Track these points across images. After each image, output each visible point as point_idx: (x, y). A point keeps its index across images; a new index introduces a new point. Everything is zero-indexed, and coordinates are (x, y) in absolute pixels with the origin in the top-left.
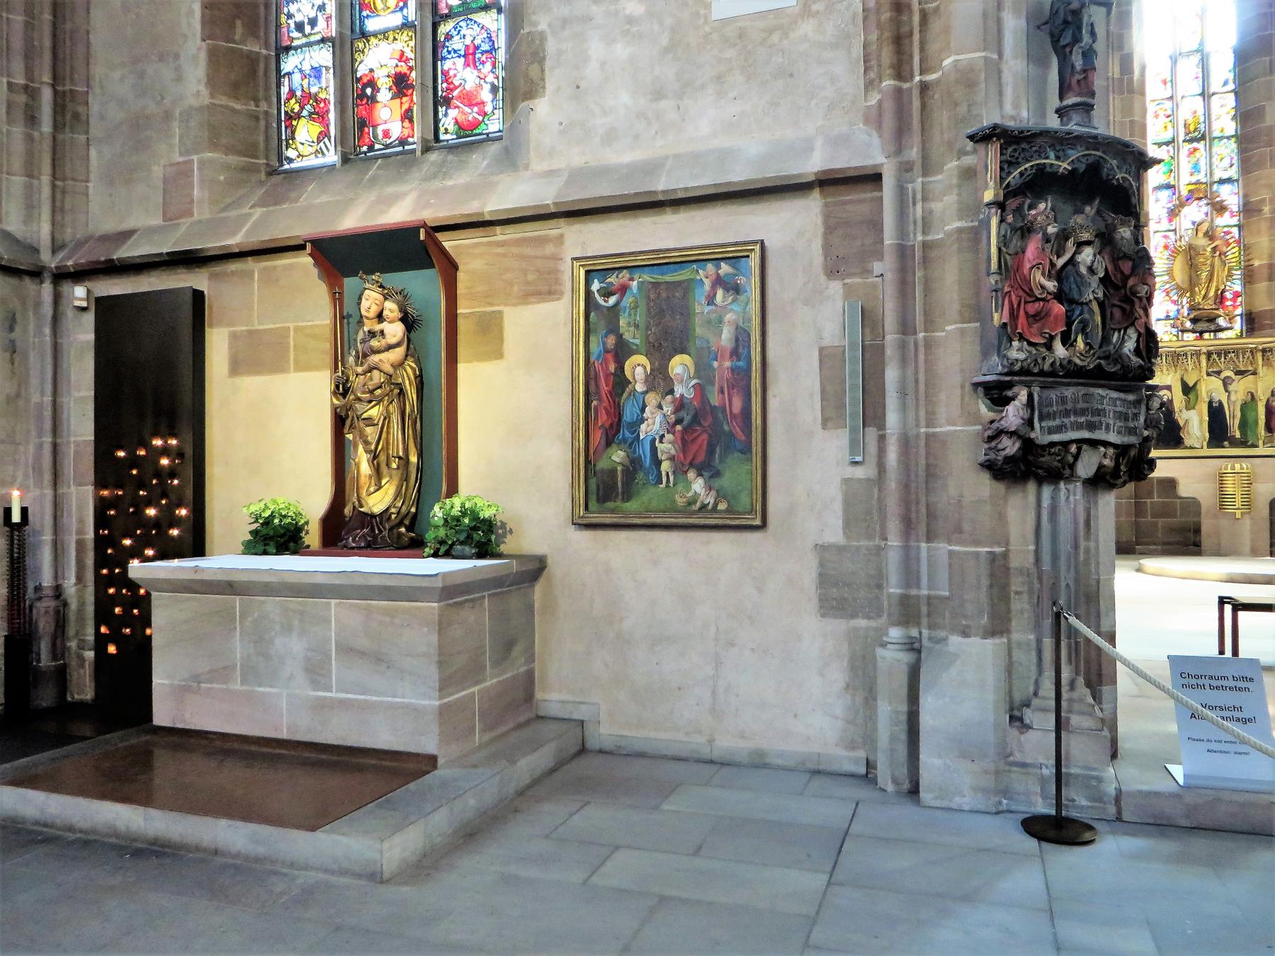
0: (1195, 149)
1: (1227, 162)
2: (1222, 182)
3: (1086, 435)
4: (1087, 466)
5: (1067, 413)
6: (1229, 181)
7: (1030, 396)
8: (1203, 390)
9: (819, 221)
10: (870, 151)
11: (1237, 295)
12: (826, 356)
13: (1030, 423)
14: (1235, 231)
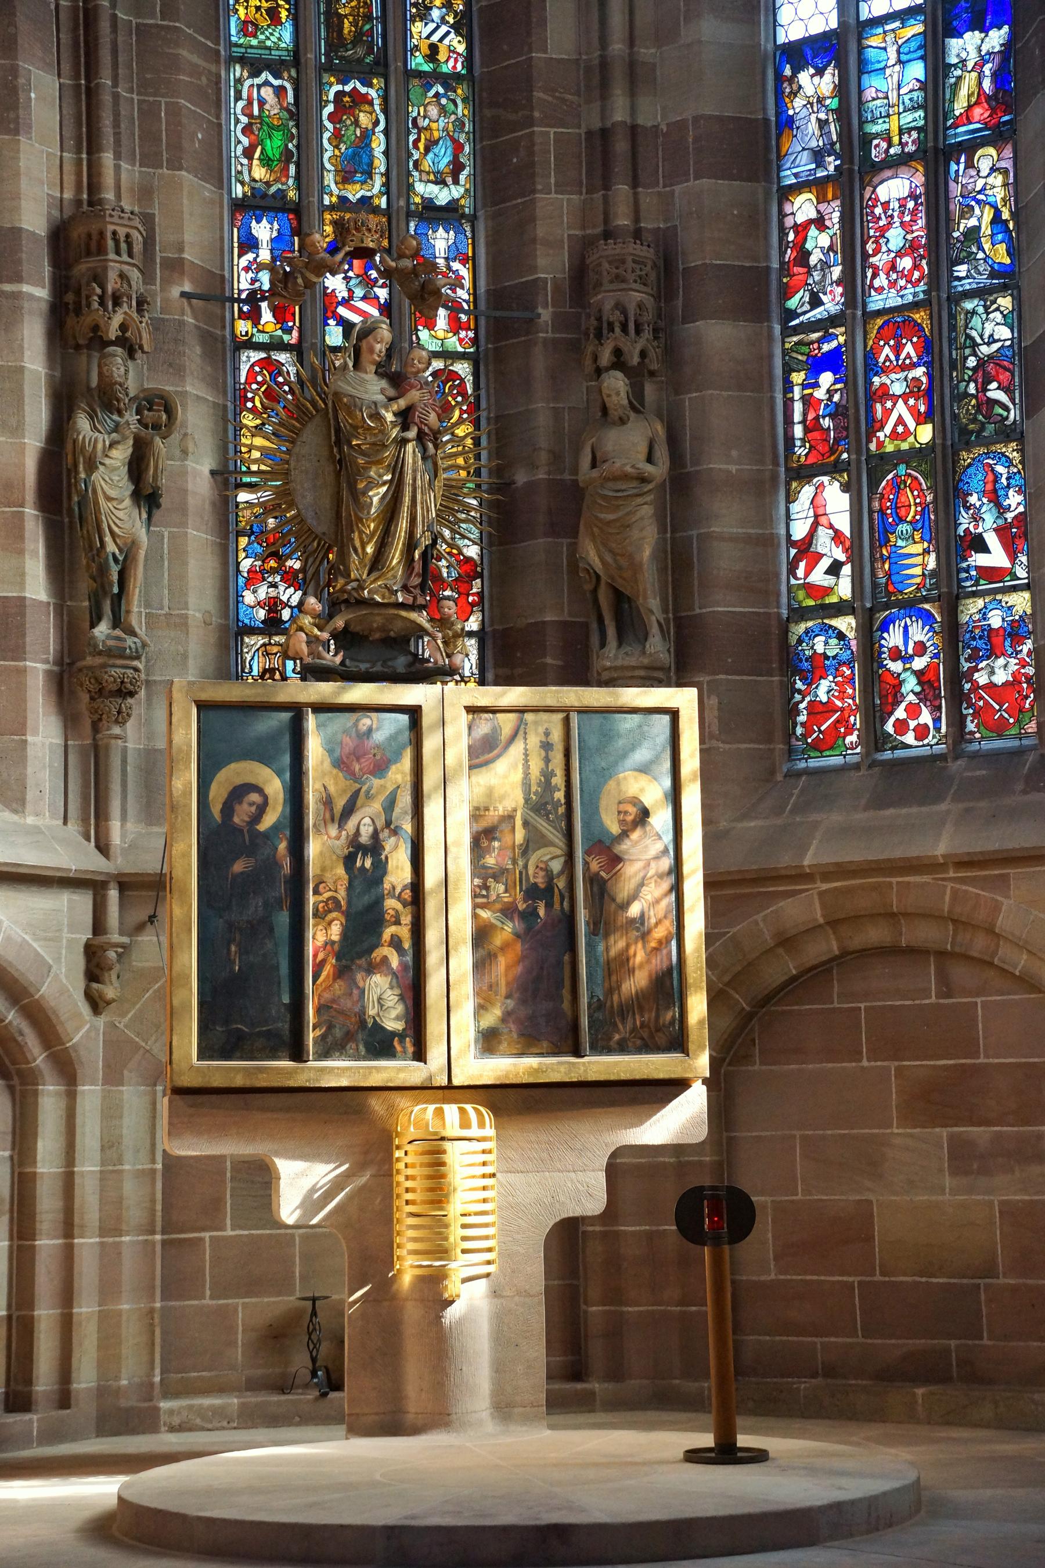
0: (359, 100)
1: (442, 157)
2: (434, 214)
11: (469, 570)
14: (462, 368)
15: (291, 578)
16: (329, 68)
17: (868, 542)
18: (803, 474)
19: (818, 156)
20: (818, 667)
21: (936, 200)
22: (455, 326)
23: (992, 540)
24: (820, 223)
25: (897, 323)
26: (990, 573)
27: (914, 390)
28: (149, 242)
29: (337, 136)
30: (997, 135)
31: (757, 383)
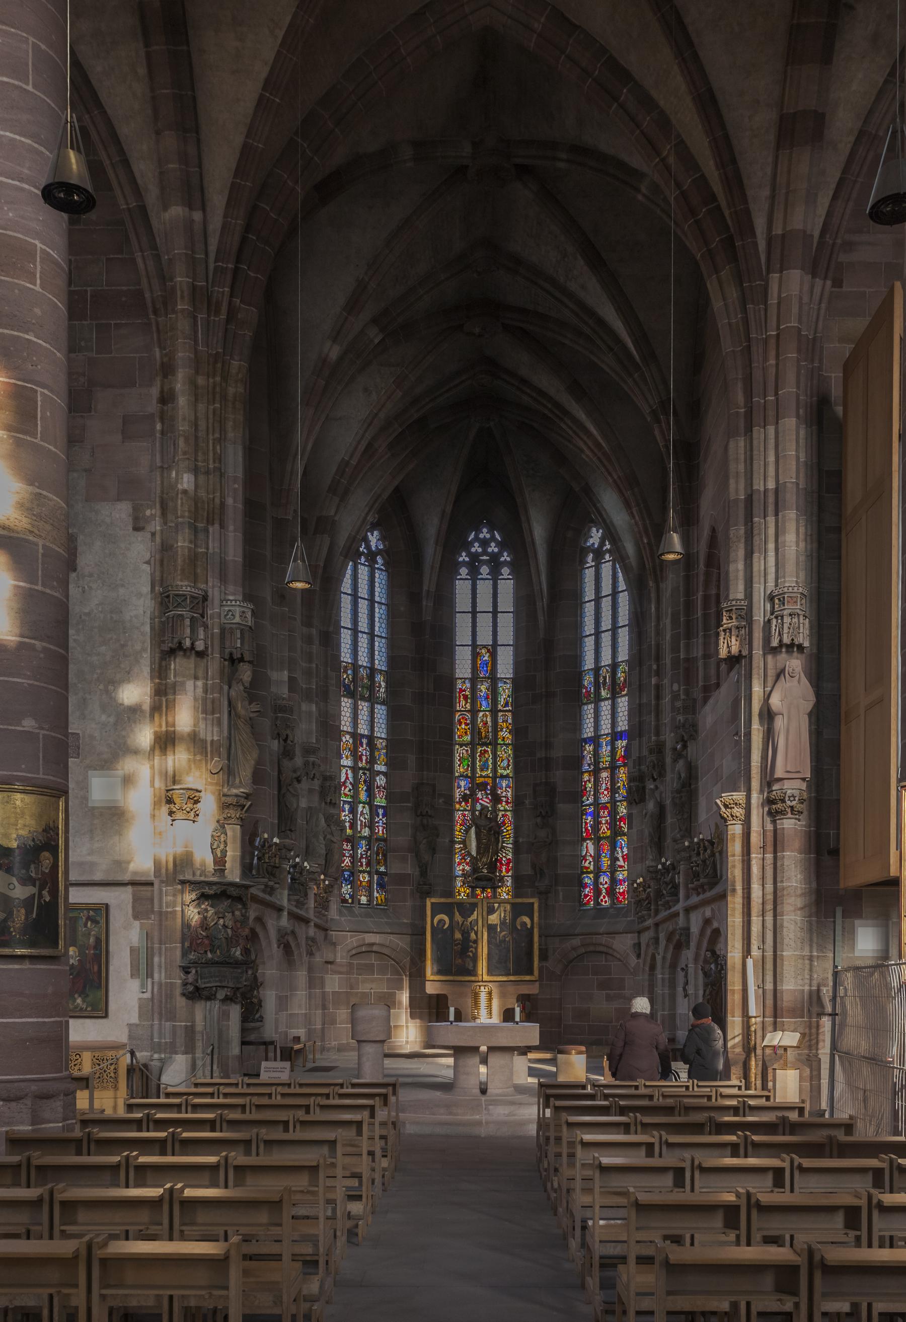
0: (486, 751)
1: (505, 763)
2: (502, 777)
3: (219, 984)
4: (221, 994)
5: (211, 977)
6: (507, 776)
7: (197, 971)
9: (131, 896)
13: (197, 981)
15: (467, 864)
16: (479, 744)
17: (597, 858)
18: (584, 840)
19: (589, 765)
21: (613, 779)
22: (507, 803)
23: (621, 859)
24: (589, 781)
26: (621, 867)
27: (607, 822)
28: (434, 791)
29: (480, 761)
30: (624, 766)
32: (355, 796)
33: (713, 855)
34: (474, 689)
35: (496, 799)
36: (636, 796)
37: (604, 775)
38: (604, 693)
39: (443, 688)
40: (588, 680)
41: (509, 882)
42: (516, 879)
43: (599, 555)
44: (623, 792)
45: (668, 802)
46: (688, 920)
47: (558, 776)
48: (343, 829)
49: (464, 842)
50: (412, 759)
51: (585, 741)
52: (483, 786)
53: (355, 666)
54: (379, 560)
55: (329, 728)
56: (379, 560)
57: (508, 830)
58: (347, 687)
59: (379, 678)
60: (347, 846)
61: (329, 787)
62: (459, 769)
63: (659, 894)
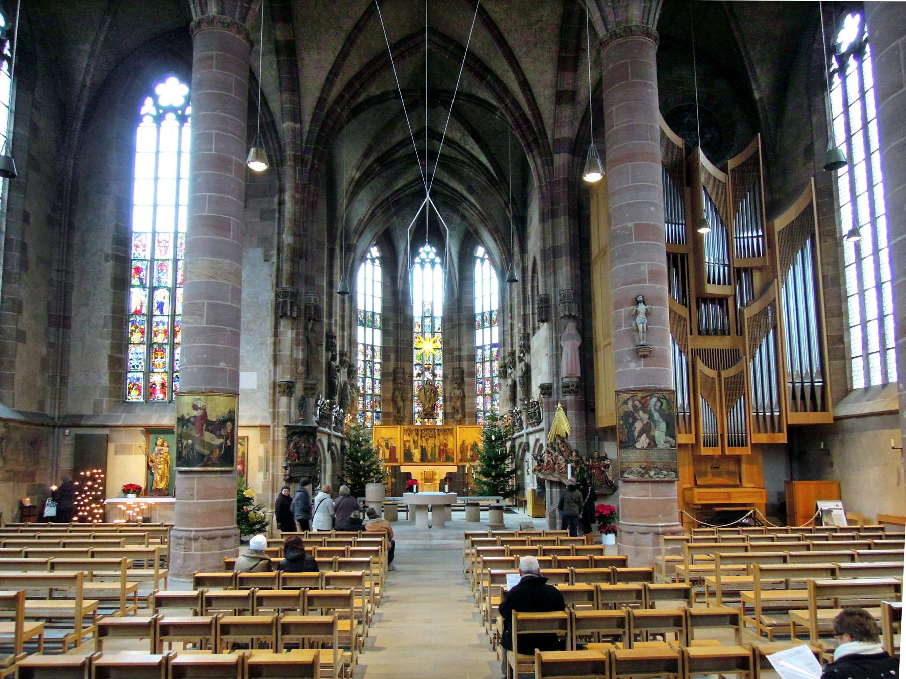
8: (419, 442)
10: (269, 422)
12: (260, 458)
17: (484, 404)
20: (479, 418)
25: (488, 379)
31: (473, 385)
32: (365, 374)
33: (538, 408)
34: (423, 321)
35: (434, 375)
36: (503, 374)
37: (487, 364)
38: (487, 324)
39: (408, 323)
40: (478, 318)
41: (441, 416)
42: (445, 414)
43: (482, 260)
44: (497, 372)
45: (518, 380)
46: (528, 438)
47: (465, 364)
48: (359, 391)
49: (418, 396)
50: (392, 356)
51: (478, 347)
52: (428, 369)
53: (365, 312)
54: (377, 261)
55: (353, 342)
56: (377, 261)
57: (440, 390)
58: (361, 321)
59: (377, 318)
60: (361, 399)
61: (352, 372)
62: (415, 361)
63: (514, 423)
